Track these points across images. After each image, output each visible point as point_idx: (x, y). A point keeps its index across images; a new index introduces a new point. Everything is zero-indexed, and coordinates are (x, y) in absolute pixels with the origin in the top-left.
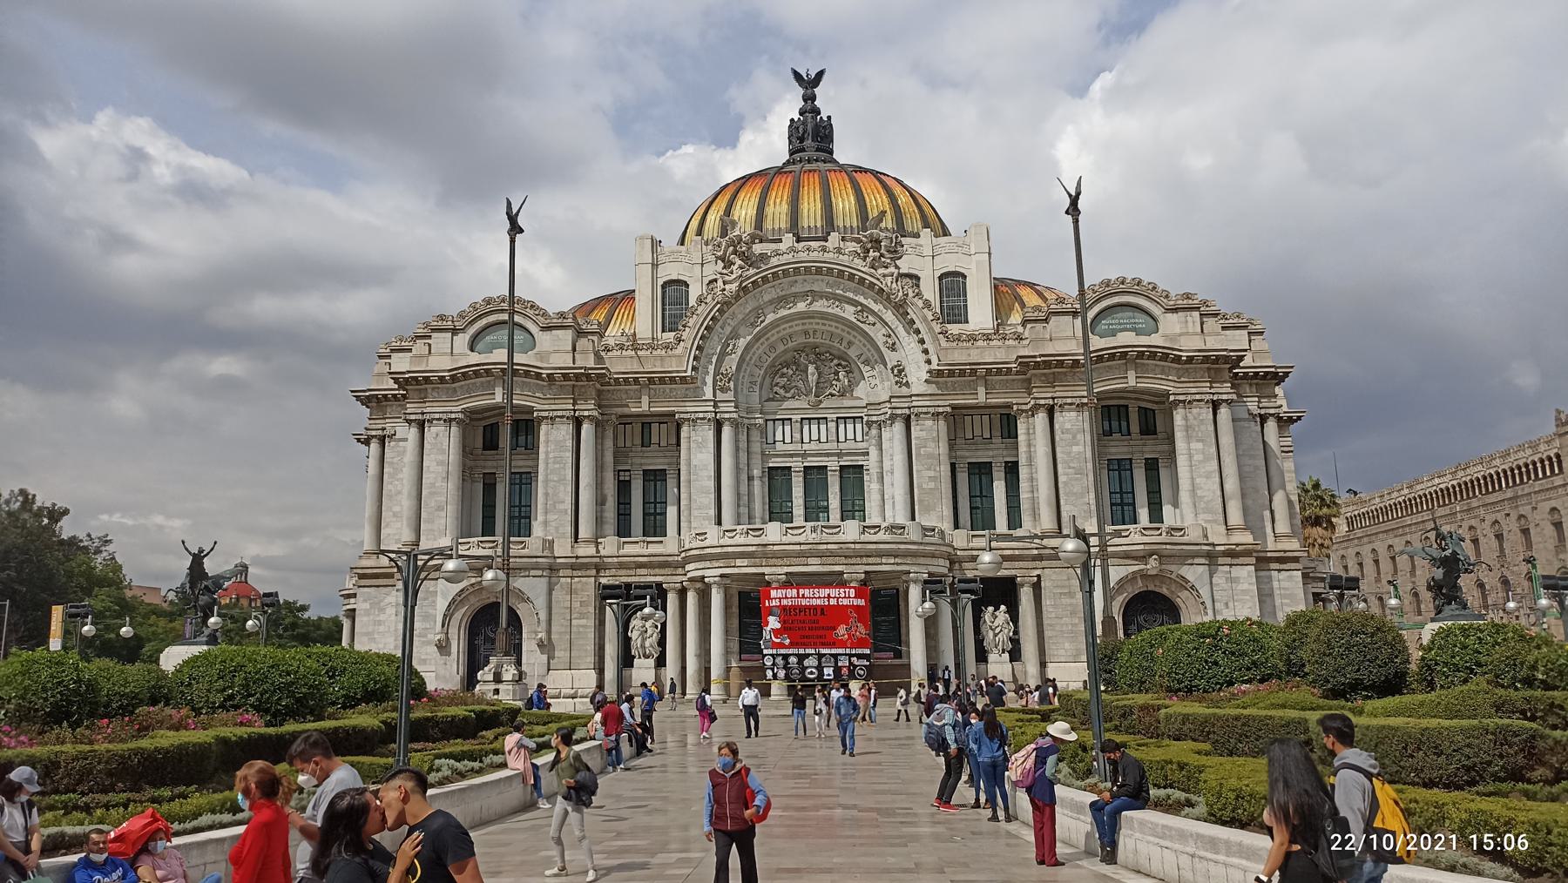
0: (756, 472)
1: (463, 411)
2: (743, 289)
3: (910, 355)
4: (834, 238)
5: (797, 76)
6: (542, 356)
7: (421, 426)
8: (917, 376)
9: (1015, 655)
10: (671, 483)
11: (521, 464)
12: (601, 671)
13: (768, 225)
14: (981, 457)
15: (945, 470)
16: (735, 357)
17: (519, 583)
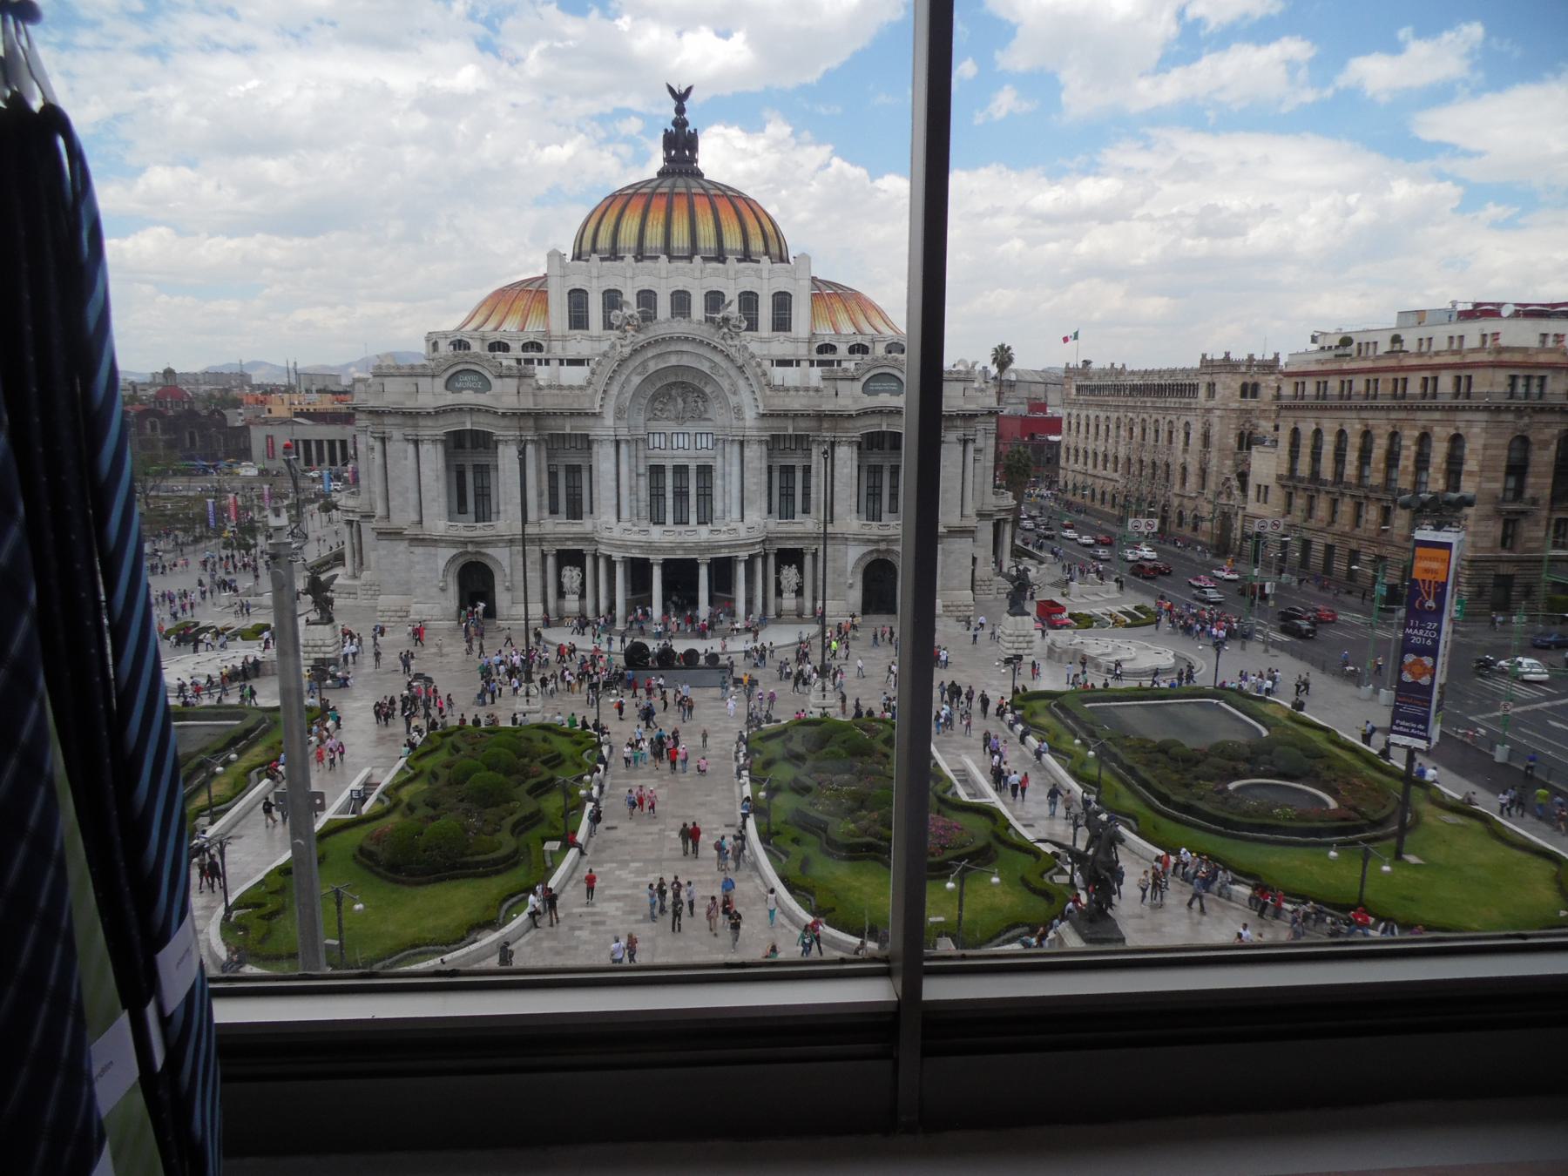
0: (642, 470)
1: (448, 434)
2: (635, 352)
3: (745, 398)
4: (697, 259)
5: (671, 90)
6: (497, 397)
7: (416, 443)
8: (750, 415)
9: (799, 592)
10: (585, 475)
11: (482, 460)
12: (545, 601)
13: (648, 243)
14: (789, 462)
15: (765, 477)
16: (628, 394)
17: (489, 551)
